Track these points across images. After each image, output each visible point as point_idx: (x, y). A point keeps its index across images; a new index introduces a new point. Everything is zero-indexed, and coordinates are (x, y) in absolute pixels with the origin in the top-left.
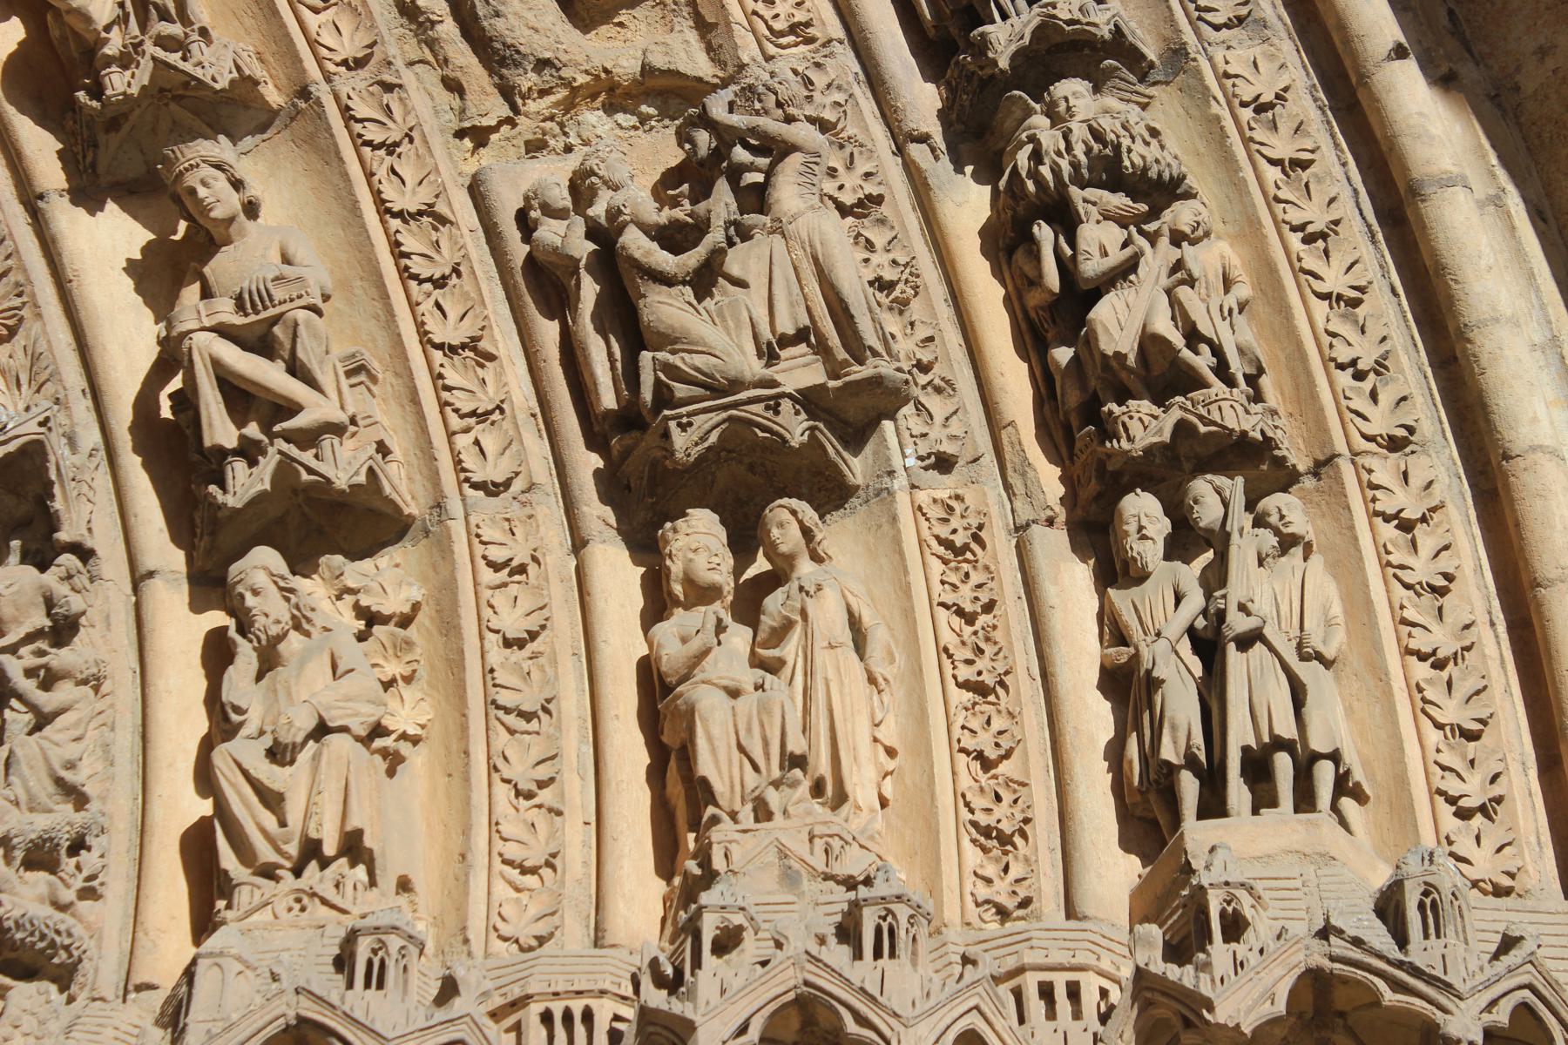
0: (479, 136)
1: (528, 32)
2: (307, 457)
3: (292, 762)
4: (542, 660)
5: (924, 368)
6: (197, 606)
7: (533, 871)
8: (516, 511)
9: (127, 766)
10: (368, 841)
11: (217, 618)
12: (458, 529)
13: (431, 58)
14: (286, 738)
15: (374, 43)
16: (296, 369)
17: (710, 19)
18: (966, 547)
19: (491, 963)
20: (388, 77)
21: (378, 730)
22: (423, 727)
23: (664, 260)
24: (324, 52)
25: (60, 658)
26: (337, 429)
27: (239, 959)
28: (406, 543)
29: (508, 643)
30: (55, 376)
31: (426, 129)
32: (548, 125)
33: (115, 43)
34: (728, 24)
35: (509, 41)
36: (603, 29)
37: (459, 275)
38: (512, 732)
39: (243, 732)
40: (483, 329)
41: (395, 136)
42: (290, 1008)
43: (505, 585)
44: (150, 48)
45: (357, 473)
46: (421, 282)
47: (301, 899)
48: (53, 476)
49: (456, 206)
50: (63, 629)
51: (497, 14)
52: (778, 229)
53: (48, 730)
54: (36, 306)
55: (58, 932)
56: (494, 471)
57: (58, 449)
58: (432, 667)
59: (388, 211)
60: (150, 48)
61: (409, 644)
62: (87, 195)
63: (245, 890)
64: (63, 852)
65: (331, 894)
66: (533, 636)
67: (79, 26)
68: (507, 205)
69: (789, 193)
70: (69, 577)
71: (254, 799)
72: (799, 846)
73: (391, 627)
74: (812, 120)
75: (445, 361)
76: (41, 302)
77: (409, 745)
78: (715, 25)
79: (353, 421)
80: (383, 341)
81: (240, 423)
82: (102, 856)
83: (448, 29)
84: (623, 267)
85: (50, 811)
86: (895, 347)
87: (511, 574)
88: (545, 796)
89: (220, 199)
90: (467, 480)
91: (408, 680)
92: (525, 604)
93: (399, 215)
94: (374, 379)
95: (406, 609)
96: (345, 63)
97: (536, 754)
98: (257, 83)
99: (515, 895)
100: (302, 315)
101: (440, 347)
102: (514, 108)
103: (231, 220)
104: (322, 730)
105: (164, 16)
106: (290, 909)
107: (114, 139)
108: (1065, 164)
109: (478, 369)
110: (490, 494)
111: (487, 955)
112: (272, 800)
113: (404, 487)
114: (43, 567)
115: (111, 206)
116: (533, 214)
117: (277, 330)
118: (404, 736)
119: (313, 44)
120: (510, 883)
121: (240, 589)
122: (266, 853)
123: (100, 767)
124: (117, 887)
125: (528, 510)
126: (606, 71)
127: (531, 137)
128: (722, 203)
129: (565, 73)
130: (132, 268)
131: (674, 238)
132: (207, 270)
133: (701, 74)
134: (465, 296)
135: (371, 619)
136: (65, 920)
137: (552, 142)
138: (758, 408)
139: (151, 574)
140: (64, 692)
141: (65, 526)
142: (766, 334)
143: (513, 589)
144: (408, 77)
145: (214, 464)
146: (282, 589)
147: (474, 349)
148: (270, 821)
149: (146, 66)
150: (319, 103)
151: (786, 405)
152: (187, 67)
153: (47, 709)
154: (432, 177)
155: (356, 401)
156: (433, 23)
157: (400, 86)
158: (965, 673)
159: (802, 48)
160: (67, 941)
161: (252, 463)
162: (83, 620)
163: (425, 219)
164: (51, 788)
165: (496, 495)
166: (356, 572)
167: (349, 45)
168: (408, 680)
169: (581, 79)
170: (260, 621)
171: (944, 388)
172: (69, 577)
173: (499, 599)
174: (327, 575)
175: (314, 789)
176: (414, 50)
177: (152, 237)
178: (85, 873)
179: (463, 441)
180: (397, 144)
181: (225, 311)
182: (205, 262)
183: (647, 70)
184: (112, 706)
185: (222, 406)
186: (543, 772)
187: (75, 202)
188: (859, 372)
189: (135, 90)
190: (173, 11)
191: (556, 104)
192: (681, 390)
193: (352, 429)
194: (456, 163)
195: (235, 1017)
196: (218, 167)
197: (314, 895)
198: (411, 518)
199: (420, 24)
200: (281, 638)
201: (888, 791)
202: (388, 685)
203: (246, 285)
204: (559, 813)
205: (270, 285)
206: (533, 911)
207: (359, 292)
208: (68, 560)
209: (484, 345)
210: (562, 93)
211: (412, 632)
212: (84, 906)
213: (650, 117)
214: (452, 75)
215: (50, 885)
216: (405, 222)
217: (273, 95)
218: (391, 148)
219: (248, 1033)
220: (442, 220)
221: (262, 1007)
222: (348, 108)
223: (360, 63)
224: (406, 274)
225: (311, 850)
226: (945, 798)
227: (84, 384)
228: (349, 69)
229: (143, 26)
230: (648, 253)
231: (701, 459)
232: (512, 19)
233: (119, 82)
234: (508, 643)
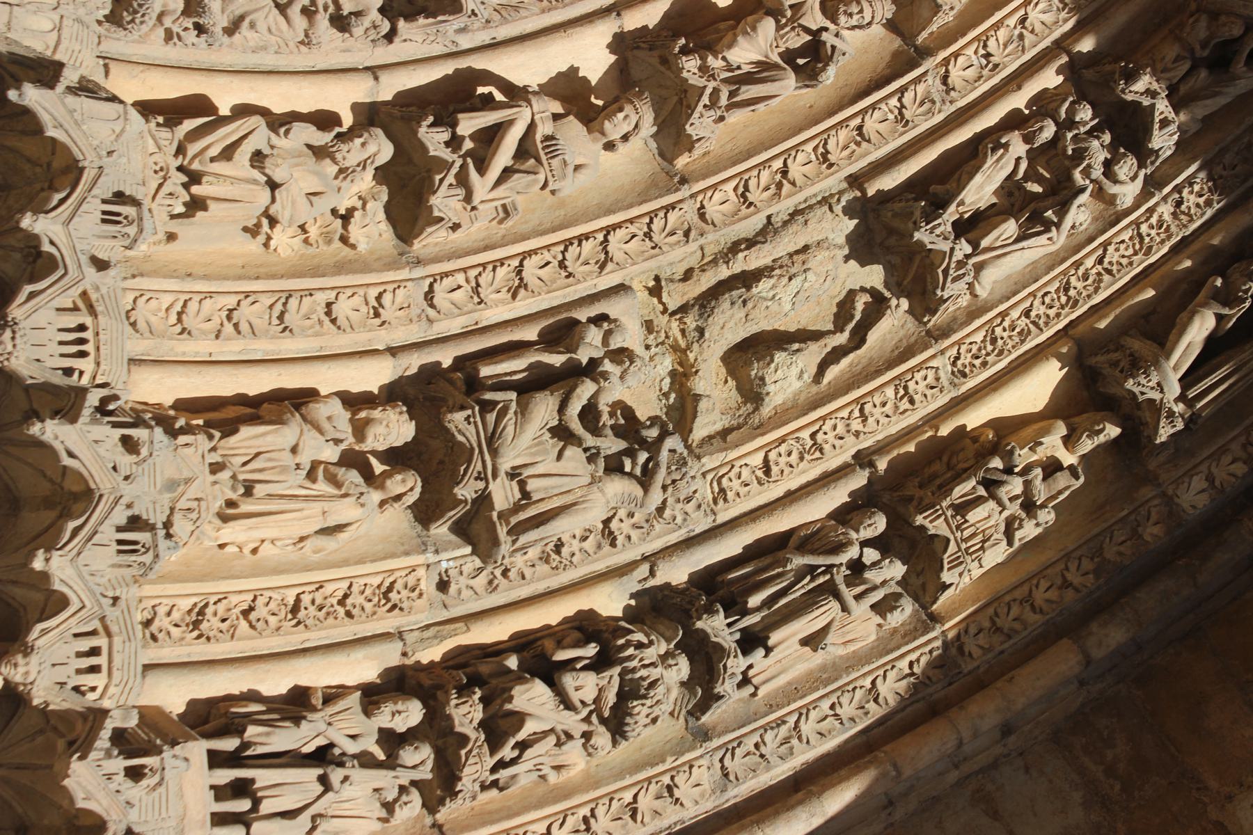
0: (656, 291)
1: (721, 322)
2: (451, 179)
3: (252, 166)
4: (317, 327)
5: (505, 573)
6: (356, 107)
7: (179, 320)
8: (415, 311)
9: (252, 61)
10: (200, 214)
11: (348, 120)
12: (404, 274)
13: (706, 261)
14: (268, 163)
15: (715, 226)
16: (507, 173)
17: (729, 438)
18: (388, 600)
19: (119, 293)
20: (693, 234)
21: (273, 222)
22: (275, 250)
23: (575, 407)
24: (709, 194)
25: (323, 20)
26: (468, 198)
27: (123, 131)
28: (395, 241)
29: (329, 305)
30: (505, 21)
31: (660, 258)
32: (663, 335)
33: (714, 63)
34: (726, 449)
35: (716, 310)
36: (724, 370)
37: (567, 277)
38: (271, 307)
39: (273, 135)
40: (533, 292)
41: (656, 238)
42: (90, 162)
43: (367, 304)
44: (712, 85)
45: (440, 210)
46: (563, 253)
47: (162, 170)
48: (440, 18)
49: (611, 276)
50: (341, 22)
51: (733, 303)
52: (594, 481)
53: (276, 11)
54: (550, 10)
55: (143, 15)
56: (440, 298)
57: (457, 22)
58: (314, 257)
59: (608, 233)
60: (712, 85)
61: (329, 242)
62: (620, 43)
63: (169, 135)
64: (196, 20)
65: (166, 189)
66: (334, 321)
67: (726, 41)
68: (612, 308)
69: (618, 488)
70: (375, 27)
71: (228, 142)
72: (193, 491)
73: (340, 231)
74: (664, 502)
75: (512, 268)
76: (552, 13)
77: (264, 241)
78: (725, 440)
79: (474, 208)
80: (525, 228)
81: (473, 137)
82: (193, 45)
83: (724, 272)
84: (571, 382)
85: (223, 12)
86: (518, 555)
87: (374, 308)
88: (229, 328)
89: (616, 126)
90: (435, 280)
91: (306, 241)
92: (354, 316)
93: (606, 240)
94: (501, 222)
95: (352, 241)
96: (702, 207)
97: (255, 322)
98: (690, 151)
99: (164, 307)
100: (541, 177)
101: (521, 265)
102: (673, 313)
103: (603, 133)
104: (273, 186)
105: (732, 94)
106: (156, 164)
107: (655, 61)
108: (634, 663)
109: (506, 288)
110: (426, 294)
111: (125, 289)
112: (228, 153)
113: (430, 240)
114: (382, 10)
115: (613, 58)
116: (605, 325)
117: (532, 161)
118: (269, 238)
119: (714, 187)
120: (172, 305)
121: (366, 135)
122: (193, 149)
123: (252, 44)
124: (173, 53)
125: (415, 319)
126: (697, 372)
127: (655, 323)
128: (611, 445)
129: (696, 346)
130: (573, 70)
131: (589, 414)
132: (571, 117)
133: (694, 432)
134: (553, 281)
135: (346, 218)
136: (151, 19)
137: (652, 337)
138: (479, 467)
139: (376, 78)
140: (300, 22)
141: (408, 25)
142: (526, 472)
143: (364, 309)
144: (693, 246)
145: (446, 120)
146: (365, 161)
147: (519, 286)
148: (214, 151)
149: (700, 82)
150: (677, 190)
151: (481, 485)
152: (700, 108)
153: (289, 11)
154: (629, 261)
155: (487, 211)
156: (727, 263)
157: (687, 242)
158: (306, 599)
159: (710, 497)
160: (137, 21)
161: (447, 144)
162: (347, 35)
163: (603, 256)
164: (238, 13)
165: (426, 299)
166: (377, 209)
167: (714, 209)
168: (306, 241)
169: (691, 356)
170: (344, 147)
171: (491, 585)
172: (375, 27)
173: (357, 300)
174: (375, 190)
175: (235, 180)
176: (711, 250)
177: (593, 83)
178: (182, 33)
180: (651, 239)
181: (544, 129)
182: (576, 117)
183: (697, 398)
184: (291, 53)
185: (484, 126)
186: (244, 327)
187: (616, 36)
188: (502, 531)
189: (685, 74)
190: (735, 100)
191: (676, 340)
192: (491, 418)
193: (469, 208)
194: (638, 276)
195: (84, 127)
196: (636, 126)
197: (165, 179)
198: (411, 245)
199: (726, 255)
201: (229, 549)
202: (302, 228)
203: (561, 142)
204: (217, 337)
205: (560, 157)
206: (153, 319)
207: (557, 213)
208: (386, 26)
209: (522, 292)
210: (683, 344)
211: (337, 244)
212: (160, 32)
213: (667, 399)
214: (695, 274)
215: (175, 11)
216: (602, 243)
217: (682, 162)
218: (648, 235)
219: (74, 135)
220: (602, 267)
221: (91, 145)
222: (674, 208)
223: (702, 216)
224: (568, 243)
225: (194, 178)
226: (224, 586)
227: (499, 39)
228: (699, 209)
229: (726, 81)
230: (579, 397)
231: (447, 431)
232: (729, 313)
233: (690, 65)
234: (329, 305)
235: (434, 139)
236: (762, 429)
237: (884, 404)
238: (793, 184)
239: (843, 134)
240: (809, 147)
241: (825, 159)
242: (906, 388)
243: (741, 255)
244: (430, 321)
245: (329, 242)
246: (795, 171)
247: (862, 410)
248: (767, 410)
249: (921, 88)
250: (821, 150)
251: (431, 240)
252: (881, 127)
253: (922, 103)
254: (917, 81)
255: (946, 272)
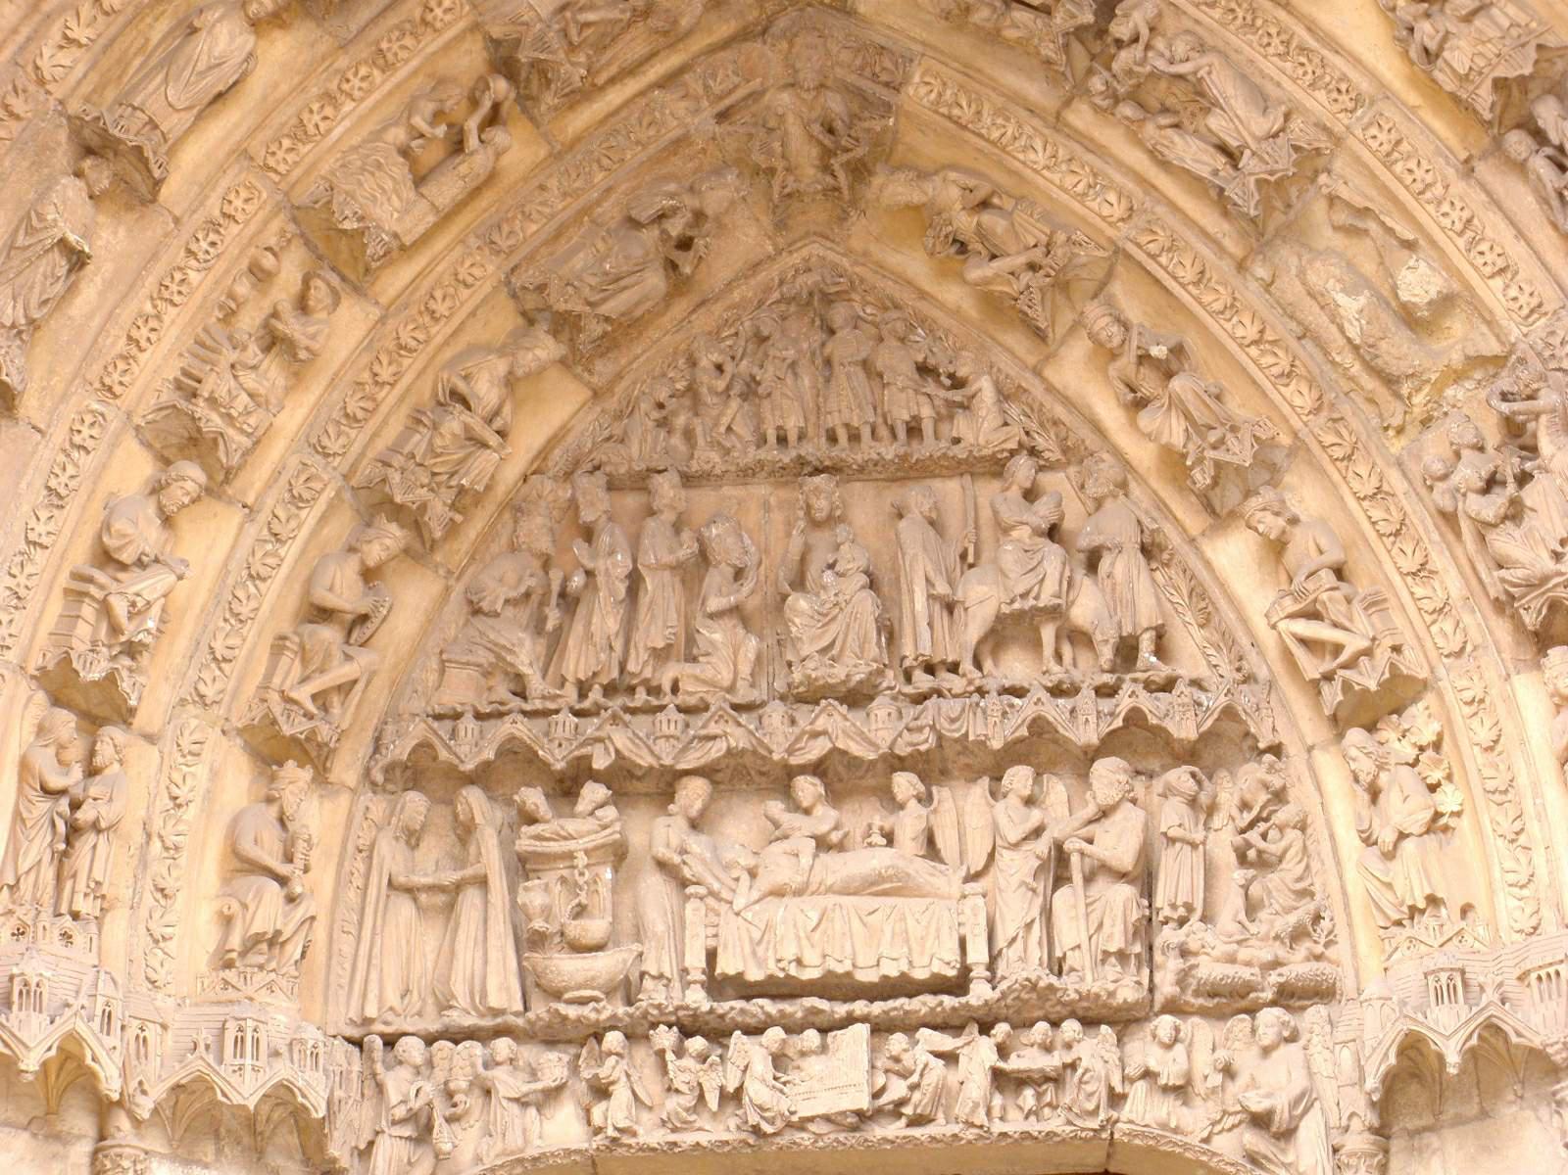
7: (1522, 887)
10: (1440, 895)
12: (1444, 684)
16: (1335, 625)
20: (1336, 416)
21: (1438, 815)
25: (1283, 815)
26: (1368, 653)
49: (1393, 481)
50: (1279, 796)
66: (1496, 742)
83: (1356, 369)
92: (1488, 723)
97: (1512, 815)
99: (1517, 903)
103: (1284, 532)
104: (1402, 836)
118: (1453, 814)
144: (1345, 409)
148: (1389, 895)
159: (1543, 320)
173: (1475, 723)
179: (1434, 629)
183: (1468, 358)
186: (1517, 825)
200: (1376, 777)
202: (1433, 788)
206: (1528, 911)
208: (1268, 758)
212: (1330, 953)
224: (1381, 536)
225: (1414, 911)
235: (1332, 694)
236: (1469, 287)
237: (1410, 171)
238: (1262, 332)
239: (1207, 298)
240: (1228, 326)
241: (1233, 306)
242: (1388, 155)
243: (1338, 359)
244: (1475, 648)
245: (1441, 761)
246: (1251, 332)
247: (1421, 193)
248: (1456, 286)
249: (1143, 239)
250: (1228, 314)
251: (1413, 663)
252: (1188, 263)
253: (1153, 232)
254: (1139, 246)
255: (1272, 173)
